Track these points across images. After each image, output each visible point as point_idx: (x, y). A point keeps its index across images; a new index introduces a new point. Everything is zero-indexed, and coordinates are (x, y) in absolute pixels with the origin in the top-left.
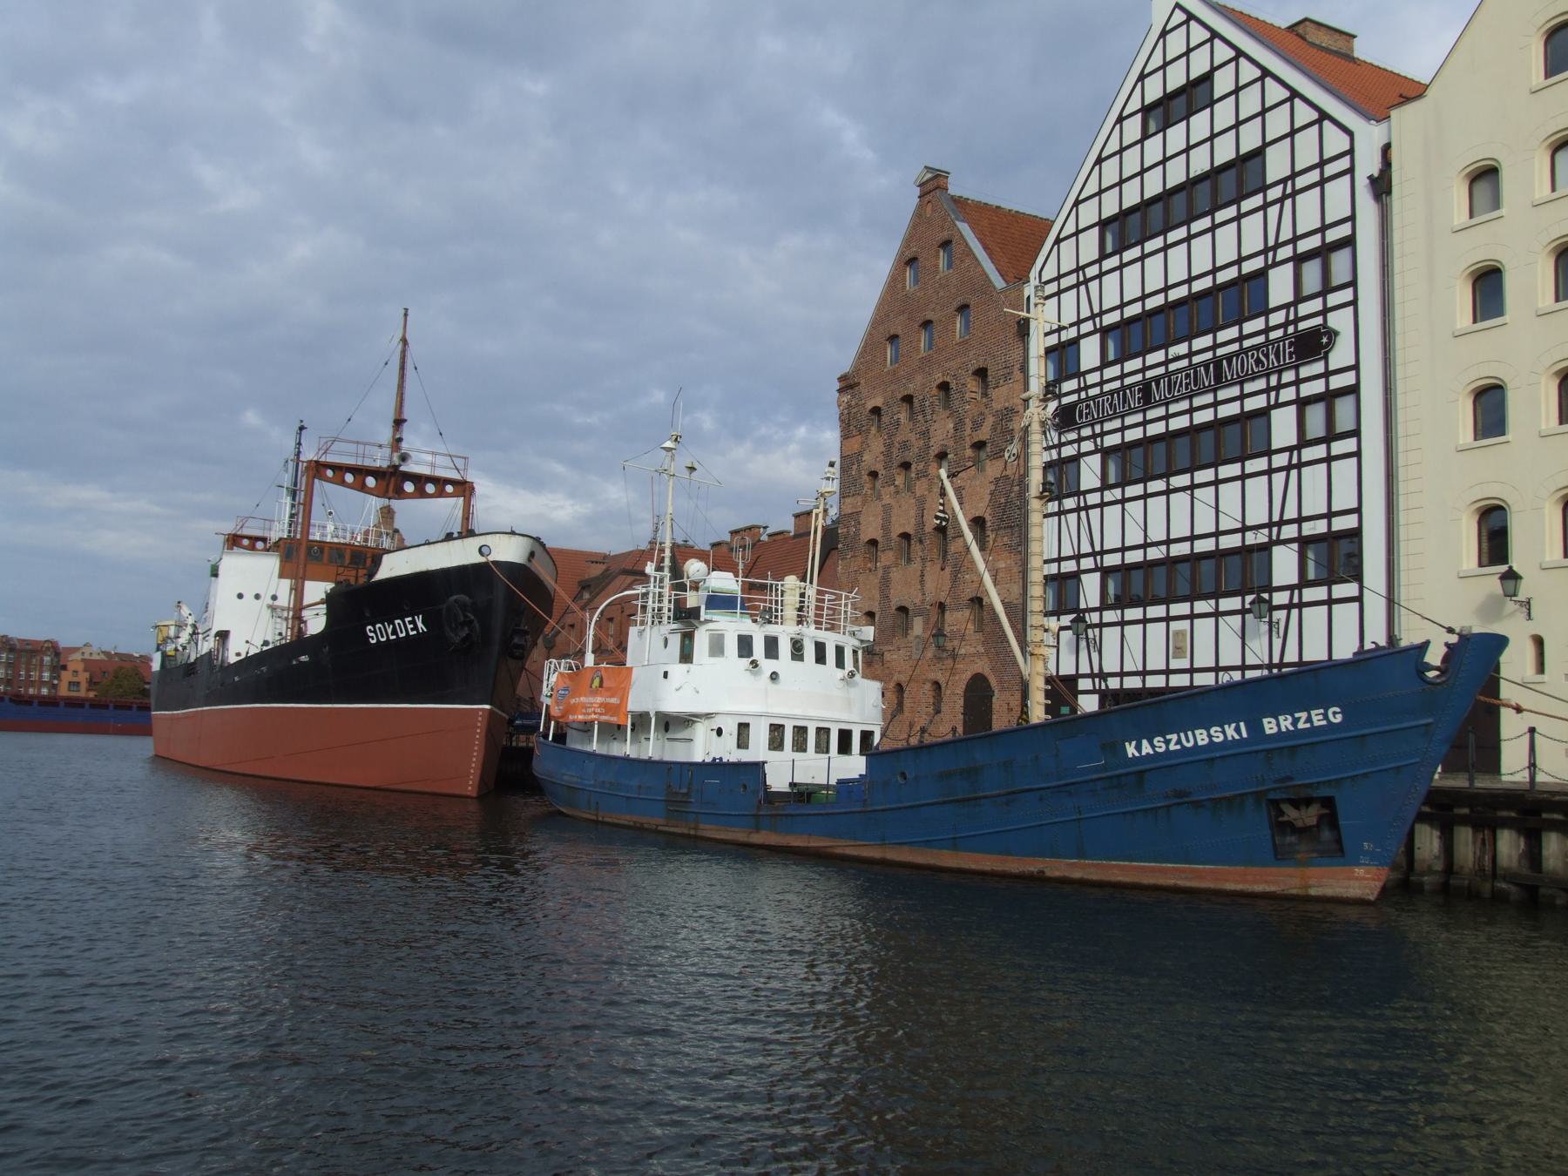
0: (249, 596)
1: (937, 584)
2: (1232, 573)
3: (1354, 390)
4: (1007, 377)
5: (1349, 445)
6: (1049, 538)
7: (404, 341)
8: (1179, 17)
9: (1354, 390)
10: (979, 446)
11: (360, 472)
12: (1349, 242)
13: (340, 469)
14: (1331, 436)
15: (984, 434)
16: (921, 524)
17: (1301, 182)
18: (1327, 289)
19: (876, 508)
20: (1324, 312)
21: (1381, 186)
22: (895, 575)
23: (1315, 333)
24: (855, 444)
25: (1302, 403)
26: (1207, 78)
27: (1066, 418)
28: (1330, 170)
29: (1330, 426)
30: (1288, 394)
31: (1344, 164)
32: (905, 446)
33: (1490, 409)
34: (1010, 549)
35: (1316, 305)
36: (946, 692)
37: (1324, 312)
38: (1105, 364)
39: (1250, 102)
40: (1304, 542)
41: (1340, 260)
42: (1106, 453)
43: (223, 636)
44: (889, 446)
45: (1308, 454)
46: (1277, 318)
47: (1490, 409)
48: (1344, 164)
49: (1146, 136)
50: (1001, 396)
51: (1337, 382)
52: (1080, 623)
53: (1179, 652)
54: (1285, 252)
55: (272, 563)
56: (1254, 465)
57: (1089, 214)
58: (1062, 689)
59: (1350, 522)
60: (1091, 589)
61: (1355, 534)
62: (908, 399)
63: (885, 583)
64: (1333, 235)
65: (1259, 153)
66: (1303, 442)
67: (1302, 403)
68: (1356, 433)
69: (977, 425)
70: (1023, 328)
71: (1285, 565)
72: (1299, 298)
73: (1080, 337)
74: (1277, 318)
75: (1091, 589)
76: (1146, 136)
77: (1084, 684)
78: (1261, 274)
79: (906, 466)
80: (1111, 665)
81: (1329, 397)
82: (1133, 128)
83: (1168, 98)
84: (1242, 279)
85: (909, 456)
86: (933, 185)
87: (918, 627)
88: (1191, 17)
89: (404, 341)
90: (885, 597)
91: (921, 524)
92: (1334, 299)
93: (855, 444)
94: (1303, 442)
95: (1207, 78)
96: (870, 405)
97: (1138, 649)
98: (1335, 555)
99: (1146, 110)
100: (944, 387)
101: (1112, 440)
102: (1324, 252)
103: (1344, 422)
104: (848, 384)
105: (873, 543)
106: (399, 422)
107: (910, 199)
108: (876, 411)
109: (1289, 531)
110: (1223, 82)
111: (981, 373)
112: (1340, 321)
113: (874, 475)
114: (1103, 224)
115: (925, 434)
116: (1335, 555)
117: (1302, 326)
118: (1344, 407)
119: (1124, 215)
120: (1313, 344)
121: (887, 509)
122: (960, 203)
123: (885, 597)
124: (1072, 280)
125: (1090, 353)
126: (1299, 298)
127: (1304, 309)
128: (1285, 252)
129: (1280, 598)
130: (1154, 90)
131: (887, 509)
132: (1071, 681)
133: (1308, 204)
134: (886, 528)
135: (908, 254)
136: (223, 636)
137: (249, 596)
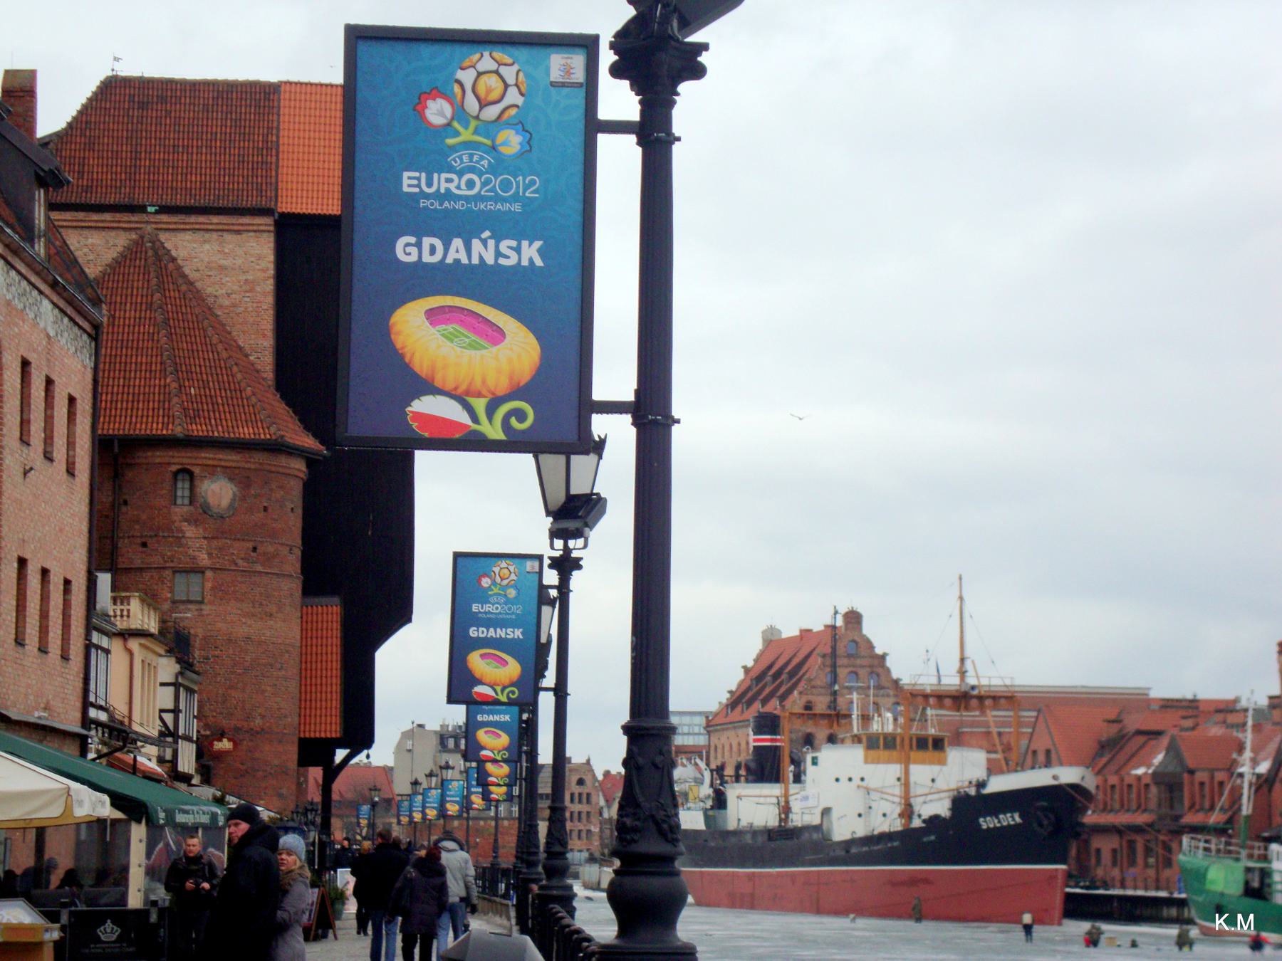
0: (844, 780)
7: (961, 598)
43: (826, 812)
89: (961, 598)
106: (962, 660)
137: (844, 780)
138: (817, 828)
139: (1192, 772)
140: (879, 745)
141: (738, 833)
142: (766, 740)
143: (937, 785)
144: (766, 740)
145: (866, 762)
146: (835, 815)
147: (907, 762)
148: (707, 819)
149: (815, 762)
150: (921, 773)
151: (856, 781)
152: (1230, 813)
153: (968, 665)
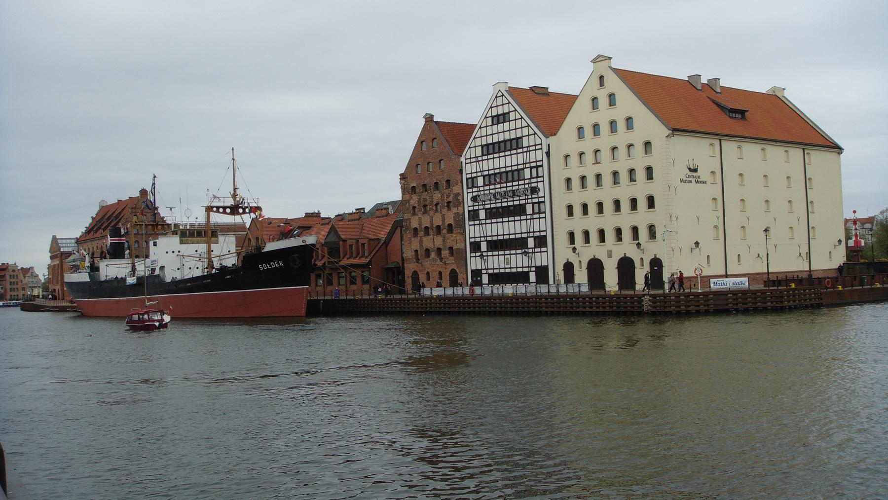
1: (439, 241)
2: (518, 244)
3: (544, 202)
4: (457, 184)
5: (543, 215)
6: (473, 231)
8: (500, 94)
9: (544, 202)
10: (449, 203)
11: (225, 208)
12: (542, 166)
13: (218, 208)
14: (539, 213)
15: (451, 199)
16: (432, 224)
17: (531, 148)
18: (537, 177)
19: (416, 218)
20: (537, 182)
21: (548, 154)
22: (425, 239)
23: (535, 188)
24: (407, 197)
25: (533, 204)
26: (508, 113)
27: (474, 199)
28: (538, 147)
29: (539, 212)
30: (530, 201)
31: (539, 147)
32: (425, 200)
33: (570, 209)
34: (461, 234)
35: (535, 180)
36: (443, 274)
37: (537, 182)
38: (485, 185)
39: (519, 122)
40: (535, 238)
41: (540, 169)
42: (486, 209)
43: (162, 268)
44: (419, 199)
45: (535, 216)
46: (527, 181)
47: (570, 209)
48: (539, 147)
49: (493, 124)
50: (456, 189)
51: (541, 200)
52: (482, 256)
53: (508, 263)
54: (528, 165)
55: (177, 239)
56: (523, 217)
57: (478, 142)
58: (477, 273)
59: (543, 234)
60: (484, 246)
61: (545, 236)
62: (424, 186)
63: (421, 241)
64: (539, 164)
65: (521, 138)
66: (534, 213)
67: (533, 204)
68: (544, 212)
69: (448, 197)
70: (461, 171)
71: (531, 243)
72: (532, 178)
73: (477, 177)
74: (527, 181)
75: (484, 246)
76: (493, 124)
77: (484, 271)
78: (523, 169)
79: (425, 206)
80: (490, 266)
81: (539, 203)
82: (489, 121)
83: (498, 116)
84: (518, 170)
85: (426, 203)
86: (429, 119)
87: (433, 255)
88: (503, 95)
90: (421, 245)
91: (432, 224)
92: (539, 179)
93: (407, 197)
94: (534, 213)
95: (508, 113)
96: (412, 185)
97: (498, 262)
98: (541, 241)
99: (493, 117)
100: (436, 183)
101: (488, 206)
102: (537, 167)
103: (542, 210)
104: (403, 177)
105: (416, 229)
107: (422, 122)
108: (414, 187)
109: (531, 235)
110: (512, 116)
111: (448, 181)
112: (540, 185)
113: (414, 207)
114: (482, 146)
115: (432, 197)
116: (541, 241)
117: (533, 185)
118: (542, 205)
119: (488, 145)
120: (535, 190)
121: (420, 219)
122: (437, 123)
123: (421, 245)
124: (474, 160)
125: (480, 182)
126: (532, 178)
127: (533, 180)
128: (528, 165)
129: (530, 251)
130: (494, 114)
131: (420, 219)
132: (481, 270)
133: (533, 153)
134: (420, 225)
135: (422, 139)
136: (162, 268)
138: (158, 276)
139: (345, 241)
140: (189, 234)
141: (106, 281)
142: (116, 240)
143: (226, 252)
144: (116, 240)
145: (181, 242)
146: (167, 270)
147: (209, 243)
148: (90, 276)
149: (155, 244)
150: (213, 246)
151: (176, 253)
152: (370, 258)
153: (238, 192)
